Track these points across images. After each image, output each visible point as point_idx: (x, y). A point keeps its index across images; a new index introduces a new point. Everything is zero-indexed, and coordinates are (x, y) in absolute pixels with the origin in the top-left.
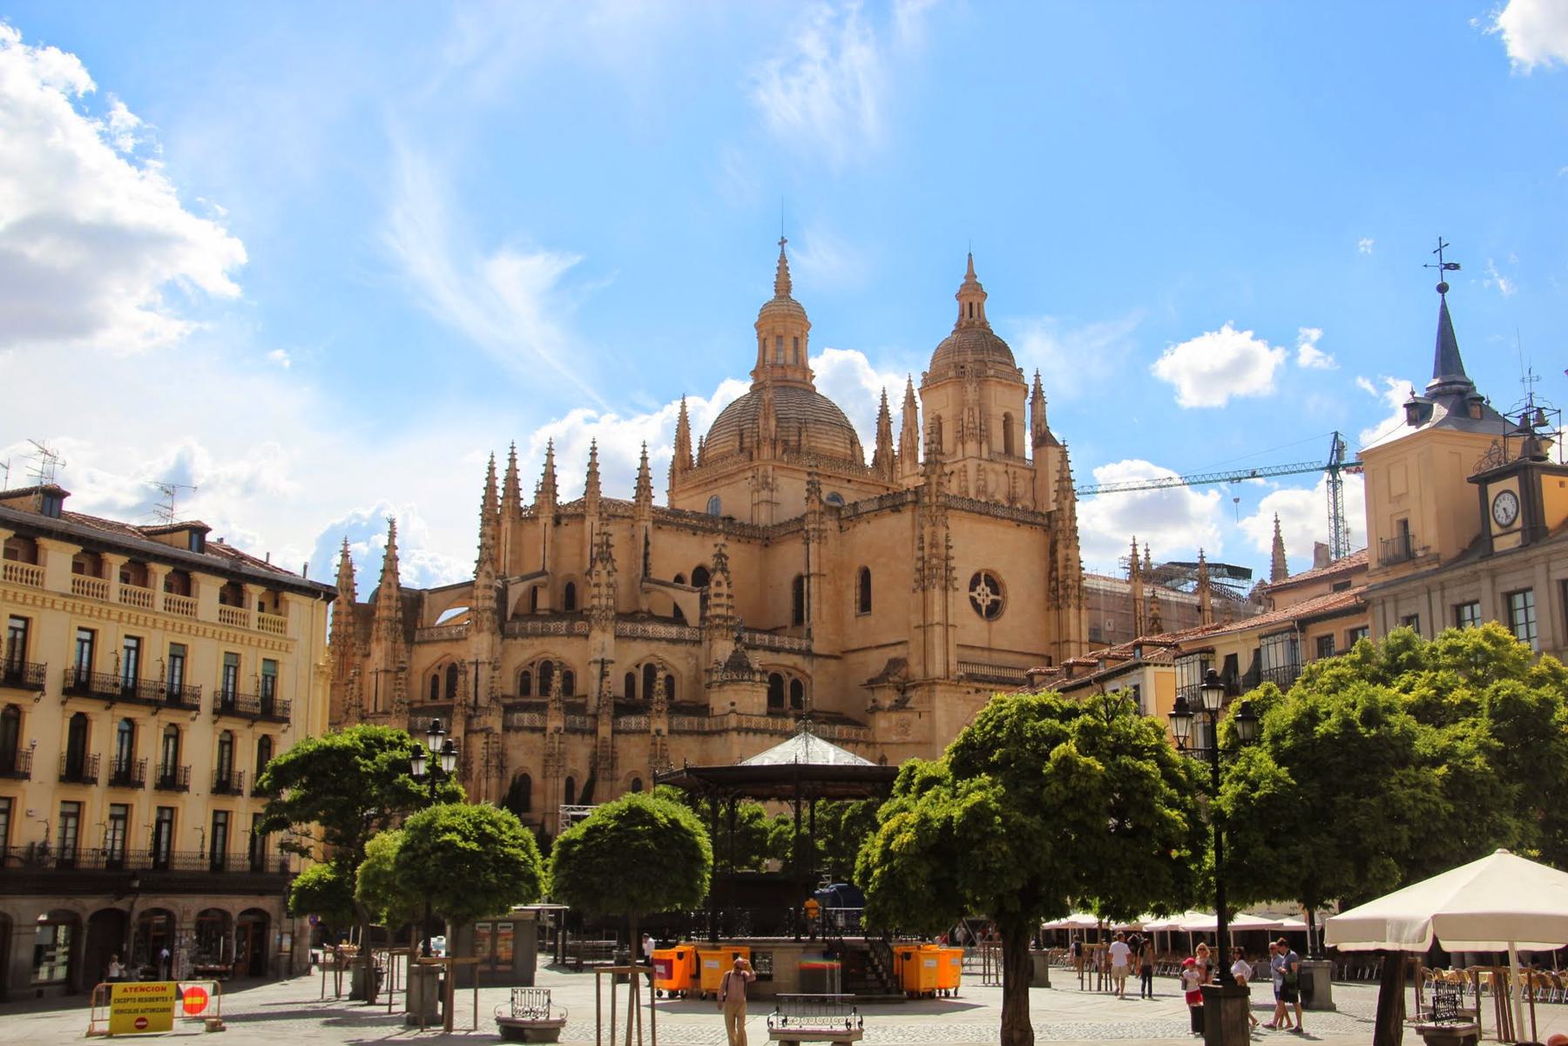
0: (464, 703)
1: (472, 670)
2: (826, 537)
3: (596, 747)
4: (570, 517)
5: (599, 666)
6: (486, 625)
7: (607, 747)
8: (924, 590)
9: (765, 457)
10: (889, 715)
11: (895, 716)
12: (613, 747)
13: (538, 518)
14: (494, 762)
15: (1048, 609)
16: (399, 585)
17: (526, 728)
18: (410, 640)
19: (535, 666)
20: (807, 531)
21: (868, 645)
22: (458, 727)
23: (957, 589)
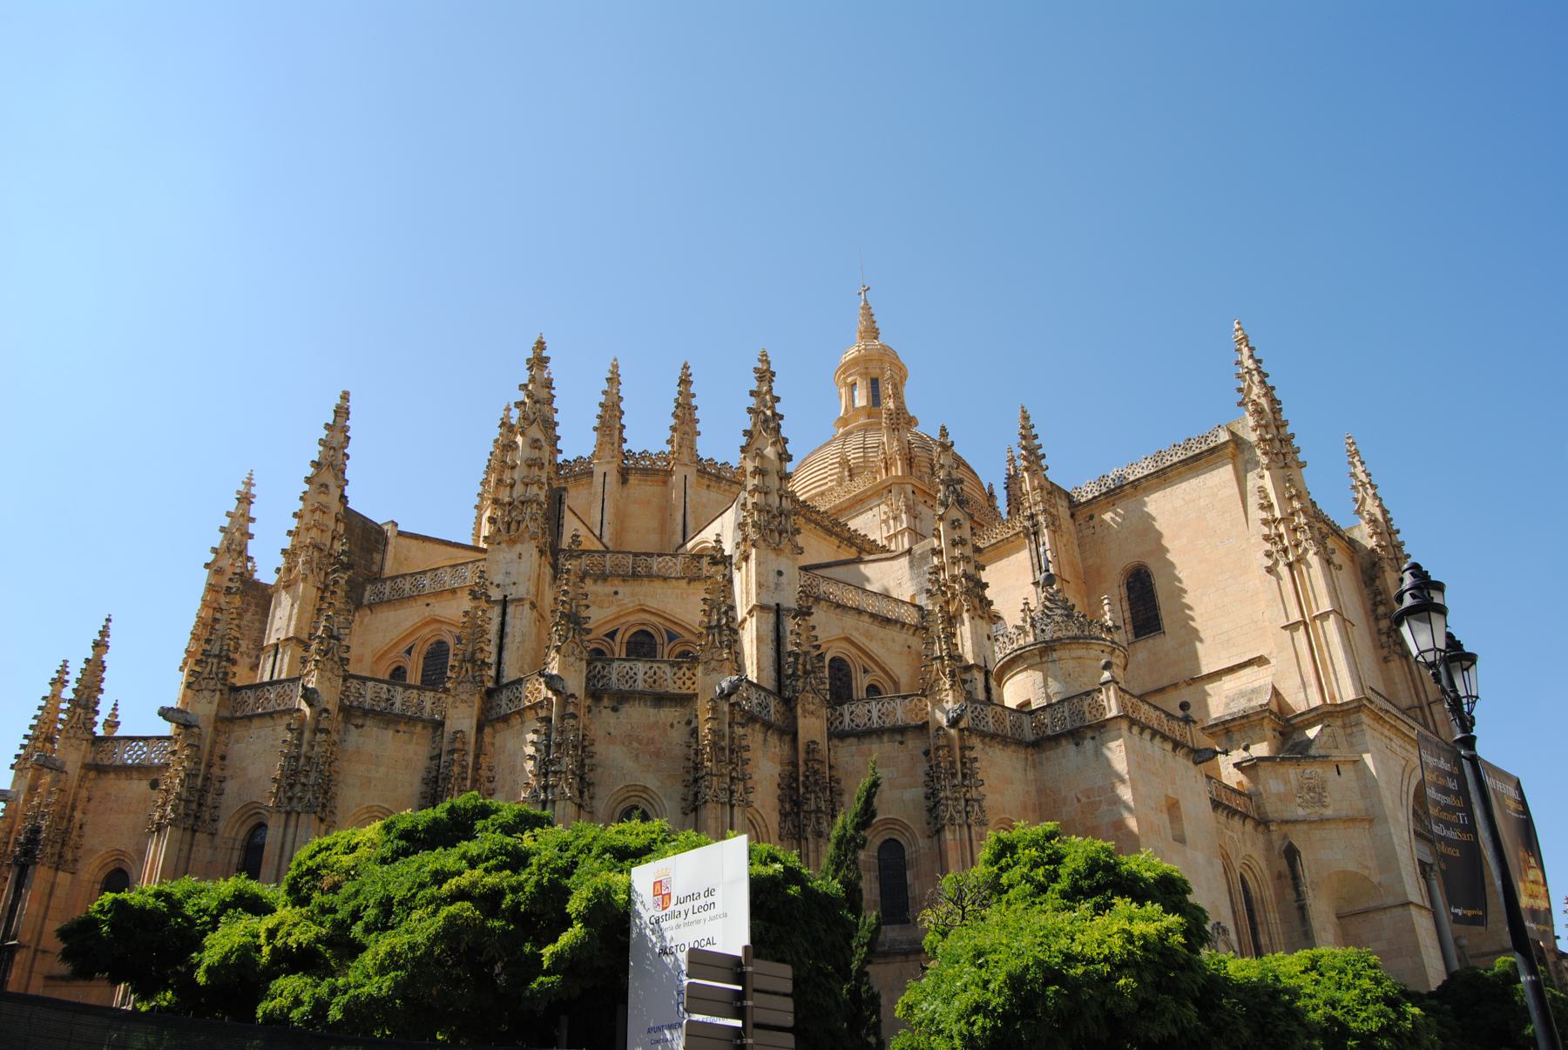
0: (479, 655)
1: (495, 613)
2: (1060, 526)
3: (795, 764)
4: (645, 471)
5: (771, 617)
6: (533, 526)
7: (822, 762)
8: (1290, 565)
9: (900, 474)
10: (1282, 770)
11: (1292, 773)
12: (831, 767)
13: (590, 473)
14: (568, 763)
15: (1386, 660)
16: (343, 499)
17: (641, 696)
18: (355, 600)
19: (618, 637)
20: (1032, 517)
21: (1165, 682)
22: (462, 707)
23: (1340, 568)
